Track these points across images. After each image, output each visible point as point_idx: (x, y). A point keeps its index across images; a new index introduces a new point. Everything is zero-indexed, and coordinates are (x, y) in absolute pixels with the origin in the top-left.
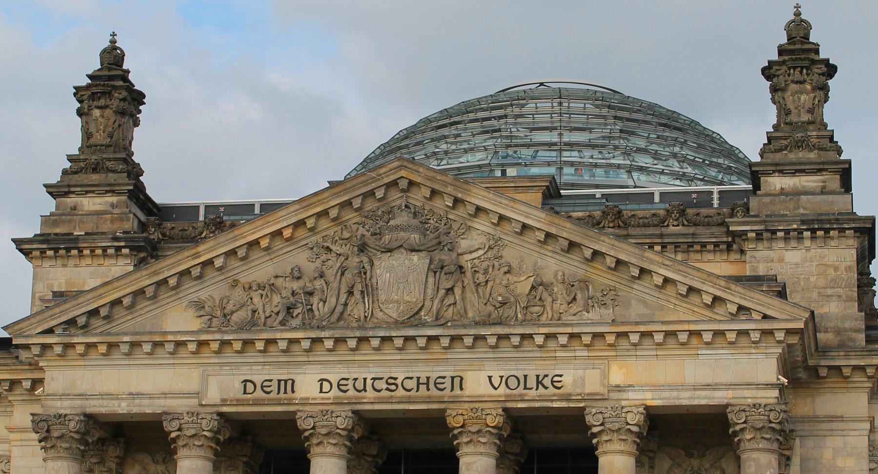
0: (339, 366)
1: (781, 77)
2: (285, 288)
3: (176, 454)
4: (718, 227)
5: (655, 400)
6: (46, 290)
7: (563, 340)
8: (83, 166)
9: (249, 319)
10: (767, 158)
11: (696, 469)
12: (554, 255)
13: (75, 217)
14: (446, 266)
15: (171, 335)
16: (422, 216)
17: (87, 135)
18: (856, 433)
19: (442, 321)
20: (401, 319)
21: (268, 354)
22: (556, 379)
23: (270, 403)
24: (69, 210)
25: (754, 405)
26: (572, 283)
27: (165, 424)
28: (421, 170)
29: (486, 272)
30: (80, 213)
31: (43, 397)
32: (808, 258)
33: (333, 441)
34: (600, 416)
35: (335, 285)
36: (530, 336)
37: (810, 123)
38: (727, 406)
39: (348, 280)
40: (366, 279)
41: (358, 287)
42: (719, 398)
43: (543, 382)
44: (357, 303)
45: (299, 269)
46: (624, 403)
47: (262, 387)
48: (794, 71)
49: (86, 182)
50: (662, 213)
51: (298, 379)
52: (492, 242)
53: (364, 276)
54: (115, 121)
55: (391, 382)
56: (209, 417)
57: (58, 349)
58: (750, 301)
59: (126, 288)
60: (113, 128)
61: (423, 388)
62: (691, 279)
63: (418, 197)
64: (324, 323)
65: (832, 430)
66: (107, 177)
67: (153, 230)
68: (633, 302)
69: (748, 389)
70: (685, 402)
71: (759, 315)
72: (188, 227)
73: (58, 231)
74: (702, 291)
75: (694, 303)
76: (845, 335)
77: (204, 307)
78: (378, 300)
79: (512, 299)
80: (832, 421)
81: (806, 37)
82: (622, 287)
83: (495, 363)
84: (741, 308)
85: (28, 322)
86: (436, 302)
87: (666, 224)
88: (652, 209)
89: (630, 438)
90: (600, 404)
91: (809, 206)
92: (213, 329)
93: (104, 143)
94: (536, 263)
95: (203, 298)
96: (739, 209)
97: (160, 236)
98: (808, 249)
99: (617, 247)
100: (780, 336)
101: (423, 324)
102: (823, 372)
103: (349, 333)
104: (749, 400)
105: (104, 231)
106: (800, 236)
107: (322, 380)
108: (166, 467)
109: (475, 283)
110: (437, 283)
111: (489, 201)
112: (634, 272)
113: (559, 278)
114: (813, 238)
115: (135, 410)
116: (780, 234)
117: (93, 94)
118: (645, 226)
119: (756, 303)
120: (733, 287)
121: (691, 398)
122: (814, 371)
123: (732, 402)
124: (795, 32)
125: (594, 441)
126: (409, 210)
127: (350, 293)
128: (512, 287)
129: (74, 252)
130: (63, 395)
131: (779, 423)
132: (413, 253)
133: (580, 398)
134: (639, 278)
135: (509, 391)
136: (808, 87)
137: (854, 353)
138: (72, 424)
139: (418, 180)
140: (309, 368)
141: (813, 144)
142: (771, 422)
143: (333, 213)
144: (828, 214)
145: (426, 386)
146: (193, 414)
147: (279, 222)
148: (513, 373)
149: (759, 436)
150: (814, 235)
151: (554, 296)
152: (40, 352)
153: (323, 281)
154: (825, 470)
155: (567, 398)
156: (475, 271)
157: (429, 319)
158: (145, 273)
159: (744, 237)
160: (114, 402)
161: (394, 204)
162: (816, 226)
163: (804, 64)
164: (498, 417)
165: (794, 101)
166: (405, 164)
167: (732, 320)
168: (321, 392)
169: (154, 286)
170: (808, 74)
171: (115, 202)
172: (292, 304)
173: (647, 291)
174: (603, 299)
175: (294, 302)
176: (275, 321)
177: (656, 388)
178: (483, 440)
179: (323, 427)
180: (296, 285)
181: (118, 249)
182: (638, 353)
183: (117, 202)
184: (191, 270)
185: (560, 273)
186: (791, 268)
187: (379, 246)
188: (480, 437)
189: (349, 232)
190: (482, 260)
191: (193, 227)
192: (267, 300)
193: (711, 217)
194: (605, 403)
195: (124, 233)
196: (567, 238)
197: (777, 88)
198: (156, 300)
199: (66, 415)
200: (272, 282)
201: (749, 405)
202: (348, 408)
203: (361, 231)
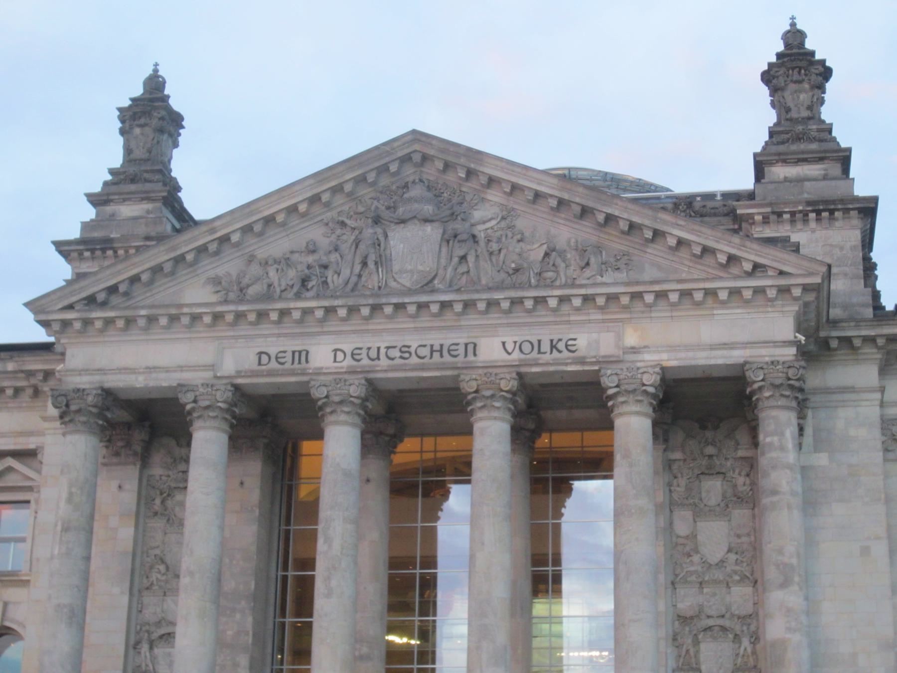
1: (781, 78)
5: (671, 360)
7: (577, 302)
11: (710, 440)
12: (568, 223)
14: (459, 234)
16: (436, 190)
17: (128, 151)
18: (868, 403)
19: (456, 287)
20: (414, 288)
22: (570, 343)
25: (772, 362)
26: (585, 249)
27: (180, 396)
29: (499, 240)
33: (346, 409)
34: (615, 378)
35: (349, 257)
37: (810, 118)
38: (746, 363)
40: (379, 250)
45: (315, 243)
46: (639, 364)
47: (277, 358)
48: (793, 71)
51: (313, 350)
52: (504, 213)
55: (405, 350)
56: (223, 388)
57: (77, 325)
58: (765, 258)
61: (436, 355)
62: (706, 238)
63: (431, 172)
64: (338, 294)
69: (764, 347)
70: (702, 362)
71: (775, 272)
74: (717, 249)
77: (220, 283)
78: (392, 271)
79: (525, 265)
80: (843, 392)
81: (802, 44)
82: (636, 252)
84: (756, 266)
89: (646, 400)
90: (614, 366)
91: (812, 190)
98: (813, 231)
99: (631, 210)
100: (797, 292)
101: (433, 291)
102: (834, 344)
103: (363, 301)
106: (806, 218)
107: (336, 350)
109: (488, 251)
110: (450, 251)
113: (572, 244)
114: (818, 220)
115: (152, 384)
116: (786, 216)
119: (772, 260)
121: (707, 358)
122: (825, 344)
123: (750, 360)
125: (610, 404)
127: (364, 264)
128: (524, 255)
129: (110, 253)
131: (798, 380)
132: (427, 224)
133: (594, 360)
134: (653, 240)
135: (523, 356)
136: (807, 86)
138: (90, 399)
141: (813, 136)
142: (789, 379)
143: (348, 187)
146: (207, 385)
150: (819, 217)
151: (567, 262)
153: (337, 255)
155: (582, 361)
156: (488, 240)
157: (440, 286)
158: (162, 248)
159: (751, 221)
161: (408, 179)
162: (821, 207)
165: (793, 99)
168: (335, 361)
171: (150, 209)
174: (616, 263)
177: (672, 348)
178: (497, 404)
179: (337, 395)
180: (310, 259)
182: (653, 315)
184: (208, 245)
185: (573, 240)
187: (392, 217)
188: (494, 401)
190: (496, 230)
193: (717, 208)
194: (620, 366)
199: (84, 390)
200: (287, 256)
201: (767, 363)
202: (360, 376)
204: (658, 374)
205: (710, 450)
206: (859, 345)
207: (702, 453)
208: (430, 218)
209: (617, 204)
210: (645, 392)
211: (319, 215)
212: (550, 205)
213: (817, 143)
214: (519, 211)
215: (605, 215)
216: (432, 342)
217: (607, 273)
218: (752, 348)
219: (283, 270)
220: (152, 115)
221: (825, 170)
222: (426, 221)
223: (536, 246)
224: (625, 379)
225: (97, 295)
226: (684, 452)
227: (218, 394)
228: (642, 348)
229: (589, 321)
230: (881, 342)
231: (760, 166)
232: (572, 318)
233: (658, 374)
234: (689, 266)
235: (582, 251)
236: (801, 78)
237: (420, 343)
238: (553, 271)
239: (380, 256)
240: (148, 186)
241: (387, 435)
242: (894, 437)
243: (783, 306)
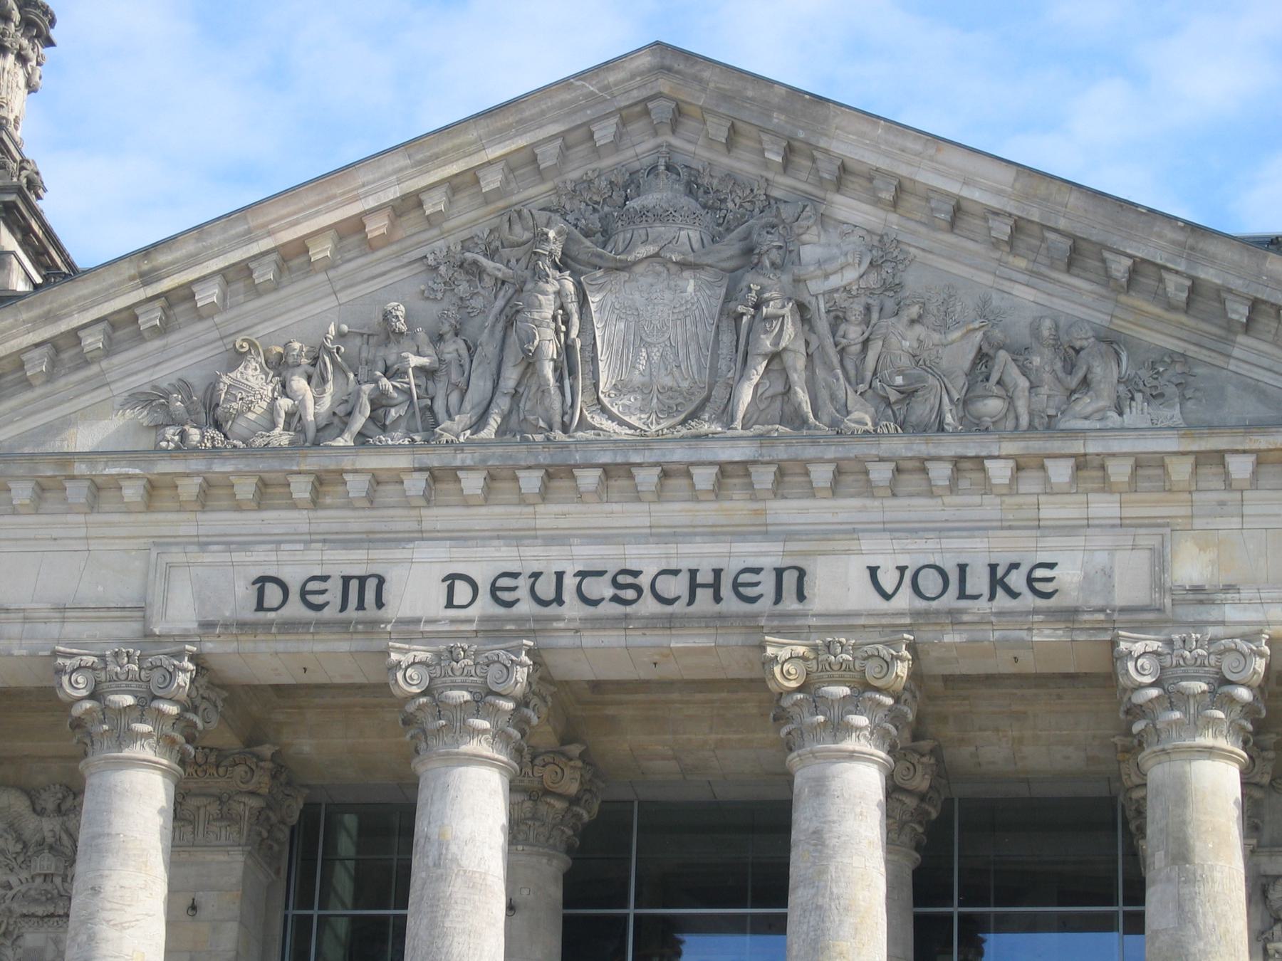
0: (496, 542)
12: (1034, 281)
15: (82, 461)
16: (706, 192)
21: (321, 513)
22: (1039, 573)
40: (567, 334)
41: (551, 349)
47: (304, 593)
51: (394, 577)
53: (563, 328)
61: (704, 595)
68: (1230, 389)
77: (165, 407)
82: (1203, 355)
94: (986, 302)
95: (165, 385)
107: (452, 578)
108: (63, 823)
112: (1235, 311)
113: (1046, 333)
126: (674, 176)
132: (686, 274)
134: (1247, 327)
135: (920, 604)
140: (423, 552)
143: (492, 181)
145: (711, 591)
147: (356, 199)
148: (931, 560)
156: (837, 317)
161: (637, 165)
166: (667, 62)
168: (450, 604)
173: (1265, 362)
185: (1047, 323)
189: (525, 229)
209: (1160, 236)
211: (419, 245)
212: (994, 234)
214: (912, 250)
215: (1129, 262)
217: (1134, 404)
222: (684, 265)
223: (956, 335)
224: (1178, 665)
241: (560, 796)
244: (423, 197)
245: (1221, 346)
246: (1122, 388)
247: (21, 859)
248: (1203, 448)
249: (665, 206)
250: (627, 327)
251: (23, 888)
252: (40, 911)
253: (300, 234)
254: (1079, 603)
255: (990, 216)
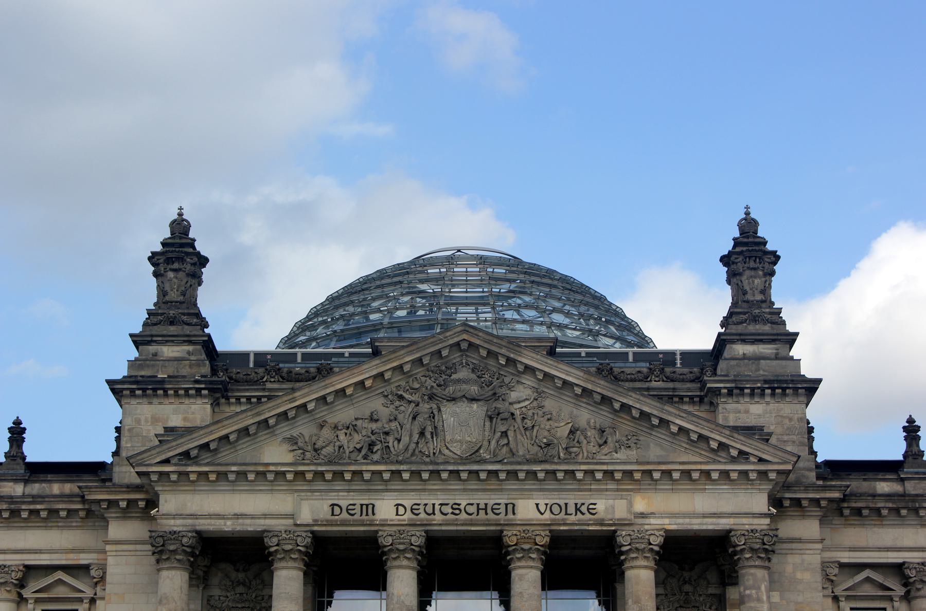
1: (739, 264)
2: (365, 428)
3: (273, 566)
4: (691, 383)
5: (672, 525)
6: (134, 423)
7: (599, 476)
8: (161, 319)
9: (336, 453)
10: (731, 329)
13: (158, 362)
14: (501, 413)
17: (162, 292)
18: (811, 552)
21: (353, 483)
22: (591, 507)
23: (355, 523)
24: (151, 356)
25: (752, 531)
26: (603, 429)
27: (266, 540)
28: (480, 334)
30: (162, 358)
31: (159, 517)
32: (768, 411)
33: (409, 556)
34: (628, 538)
35: (408, 426)
36: (573, 472)
37: (763, 302)
38: (730, 531)
39: (420, 422)
40: (434, 422)
41: (429, 429)
42: (722, 524)
43: (580, 509)
44: (427, 443)
46: (646, 527)
47: (347, 510)
48: (749, 260)
49: (165, 333)
50: (645, 370)
51: (378, 504)
54: (187, 282)
55: (456, 507)
58: (749, 447)
59: (233, 426)
60: (185, 287)
61: (482, 512)
63: (474, 358)
64: (400, 458)
65: (792, 549)
66: (183, 328)
67: (222, 374)
68: (652, 445)
70: (696, 527)
72: (251, 372)
73: (143, 373)
74: (711, 438)
75: (702, 447)
76: (800, 473)
77: (296, 443)
79: (556, 441)
80: (792, 542)
83: (542, 493)
84: (741, 453)
85: (149, 454)
86: (493, 443)
87: (649, 380)
88: (638, 367)
90: (627, 528)
91: (768, 369)
92: (306, 462)
93: (179, 299)
95: (295, 435)
96: (708, 369)
97: (227, 379)
98: (768, 403)
99: (642, 401)
100: (772, 476)
101: (484, 461)
103: (424, 467)
104: (747, 526)
105: (183, 374)
107: (398, 505)
109: (524, 427)
110: (493, 427)
111: (537, 361)
114: (773, 395)
115: (239, 528)
116: (747, 391)
117: (168, 258)
118: (632, 380)
119: (754, 449)
120: (736, 435)
121: (701, 524)
124: (748, 228)
125: (623, 557)
126: (468, 366)
127: (422, 434)
129: (160, 392)
130: (176, 515)
132: (473, 402)
133: (611, 522)
134: (657, 427)
136: (761, 273)
137: (811, 489)
139: (478, 342)
141: (767, 318)
144: (784, 376)
145: (484, 511)
146: (290, 532)
147: (362, 374)
149: (755, 556)
152: (158, 478)
154: (787, 581)
155: (601, 523)
156: (523, 417)
160: (220, 521)
161: (454, 361)
162: (776, 385)
163: (752, 254)
164: (546, 537)
165: (749, 283)
167: (734, 462)
168: (397, 514)
169: (256, 425)
170: (760, 263)
171: (191, 350)
172: (373, 442)
174: (627, 442)
175: (375, 440)
176: (358, 456)
177: (672, 515)
178: (534, 556)
179: (400, 544)
180: (374, 426)
181: (198, 390)
183: (193, 350)
184: (287, 412)
185: (593, 421)
186: (755, 418)
187: (445, 395)
188: (531, 553)
189: (418, 383)
190: (528, 408)
191: (256, 373)
192: (350, 438)
193: (684, 374)
194: (631, 528)
195: (202, 376)
196: (601, 392)
197: (736, 273)
198: (256, 436)
199: (179, 532)
200: (354, 423)
201: (748, 531)
203: (429, 383)
204: (662, 536)
205: (687, 588)
206: (807, 505)
207: (680, 590)
208: (477, 398)
209: (631, 396)
210: (652, 550)
212: (576, 392)
213: (769, 325)
215: (621, 403)
216: (478, 502)
218: (735, 517)
219: (350, 433)
220: (185, 260)
221: (777, 349)
222: (473, 400)
225: (190, 451)
226: (665, 589)
227: (299, 539)
228: (650, 514)
229: (607, 490)
230: (823, 503)
231: (721, 342)
232: (593, 487)
233: (662, 536)
234: (686, 448)
235: (602, 431)
236: (756, 266)
237: (468, 502)
238: (577, 447)
239: (436, 428)
240: (187, 330)
242: (828, 577)
243: (760, 484)
244: (384, 373)
245: (649, 431)
246: (617, 444)
247: (231, 587)
248: (645, 469)
249: (466, 378)
250: (454, 420)
251: (233, 598)
252: (240, 606)
253: (343, 386)
254: (604, 517)
255: (574, 385)
